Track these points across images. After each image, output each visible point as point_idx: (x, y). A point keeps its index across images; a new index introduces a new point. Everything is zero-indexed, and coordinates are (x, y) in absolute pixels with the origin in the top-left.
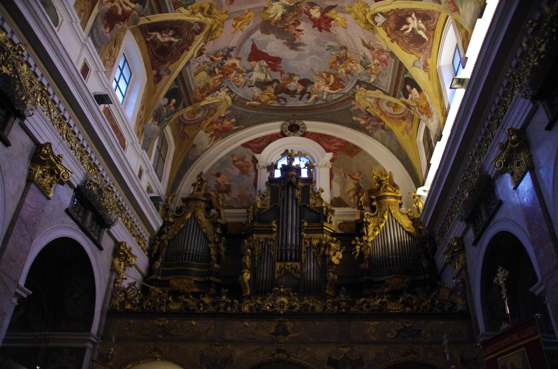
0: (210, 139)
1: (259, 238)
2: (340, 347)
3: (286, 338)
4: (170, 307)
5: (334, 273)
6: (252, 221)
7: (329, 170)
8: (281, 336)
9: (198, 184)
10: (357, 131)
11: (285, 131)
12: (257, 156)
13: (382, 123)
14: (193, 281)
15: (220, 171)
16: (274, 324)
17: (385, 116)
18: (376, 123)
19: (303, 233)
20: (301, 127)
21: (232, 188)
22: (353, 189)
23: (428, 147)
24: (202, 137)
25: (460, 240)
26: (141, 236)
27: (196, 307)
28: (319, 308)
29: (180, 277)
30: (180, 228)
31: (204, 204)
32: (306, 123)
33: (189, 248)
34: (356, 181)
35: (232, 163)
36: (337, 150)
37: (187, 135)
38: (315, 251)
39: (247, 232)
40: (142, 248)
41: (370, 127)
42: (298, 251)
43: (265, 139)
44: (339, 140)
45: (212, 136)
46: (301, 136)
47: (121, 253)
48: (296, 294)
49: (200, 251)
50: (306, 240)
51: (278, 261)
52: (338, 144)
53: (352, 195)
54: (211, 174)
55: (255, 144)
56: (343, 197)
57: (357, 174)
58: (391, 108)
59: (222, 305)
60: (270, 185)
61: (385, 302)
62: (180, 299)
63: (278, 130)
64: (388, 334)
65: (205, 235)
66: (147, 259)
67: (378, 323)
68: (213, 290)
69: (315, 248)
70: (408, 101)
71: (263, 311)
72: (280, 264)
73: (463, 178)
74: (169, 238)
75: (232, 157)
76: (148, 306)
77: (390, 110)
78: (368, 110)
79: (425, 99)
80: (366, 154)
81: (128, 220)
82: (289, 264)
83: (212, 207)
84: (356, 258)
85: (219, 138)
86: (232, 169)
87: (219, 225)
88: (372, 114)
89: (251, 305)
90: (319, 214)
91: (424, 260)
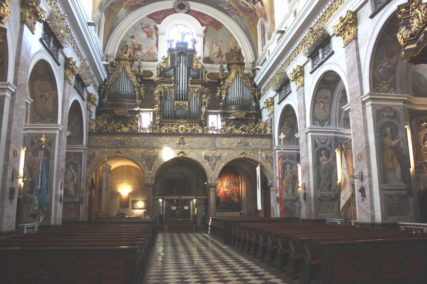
1: (164, 86)
5: (206, 108)
6: (160, 76)
9: (125, 49)
15: (134, 35)
16: (178, 139)
17: (240, 8)
18: (234, 11)
19: (189, 84)
21: (142, 47)
24: (123, 11)
25: (272, 99)
29: (120, 108)
32: (191, 3)
33: (123, 91)
34: (218, 47)
37: (113, 11)
38: (196, 95)
44: (210, 17)
45: (128, 10)
46: (185, 13)
50: (191, 89)
51: (175, 100)
52: (209, 20)
56: (210, 58)
57: (219, 42)
58: (244, 5)
60: (170, 53)
61: (233, 129)
62: (128, 126)
63: (171, 7)
65: (131, 82)
70: (255, 7)
72: (176, 102)
73: (277, 72)
75: (141, 24)
76: (110, 130)
77: (244, 6)
78: (230, 3)
79: (265, 10)
80: (226, 29)
82: (181, 102)
86: (142, 34)
88: (232, 5)
89: (166, 129)
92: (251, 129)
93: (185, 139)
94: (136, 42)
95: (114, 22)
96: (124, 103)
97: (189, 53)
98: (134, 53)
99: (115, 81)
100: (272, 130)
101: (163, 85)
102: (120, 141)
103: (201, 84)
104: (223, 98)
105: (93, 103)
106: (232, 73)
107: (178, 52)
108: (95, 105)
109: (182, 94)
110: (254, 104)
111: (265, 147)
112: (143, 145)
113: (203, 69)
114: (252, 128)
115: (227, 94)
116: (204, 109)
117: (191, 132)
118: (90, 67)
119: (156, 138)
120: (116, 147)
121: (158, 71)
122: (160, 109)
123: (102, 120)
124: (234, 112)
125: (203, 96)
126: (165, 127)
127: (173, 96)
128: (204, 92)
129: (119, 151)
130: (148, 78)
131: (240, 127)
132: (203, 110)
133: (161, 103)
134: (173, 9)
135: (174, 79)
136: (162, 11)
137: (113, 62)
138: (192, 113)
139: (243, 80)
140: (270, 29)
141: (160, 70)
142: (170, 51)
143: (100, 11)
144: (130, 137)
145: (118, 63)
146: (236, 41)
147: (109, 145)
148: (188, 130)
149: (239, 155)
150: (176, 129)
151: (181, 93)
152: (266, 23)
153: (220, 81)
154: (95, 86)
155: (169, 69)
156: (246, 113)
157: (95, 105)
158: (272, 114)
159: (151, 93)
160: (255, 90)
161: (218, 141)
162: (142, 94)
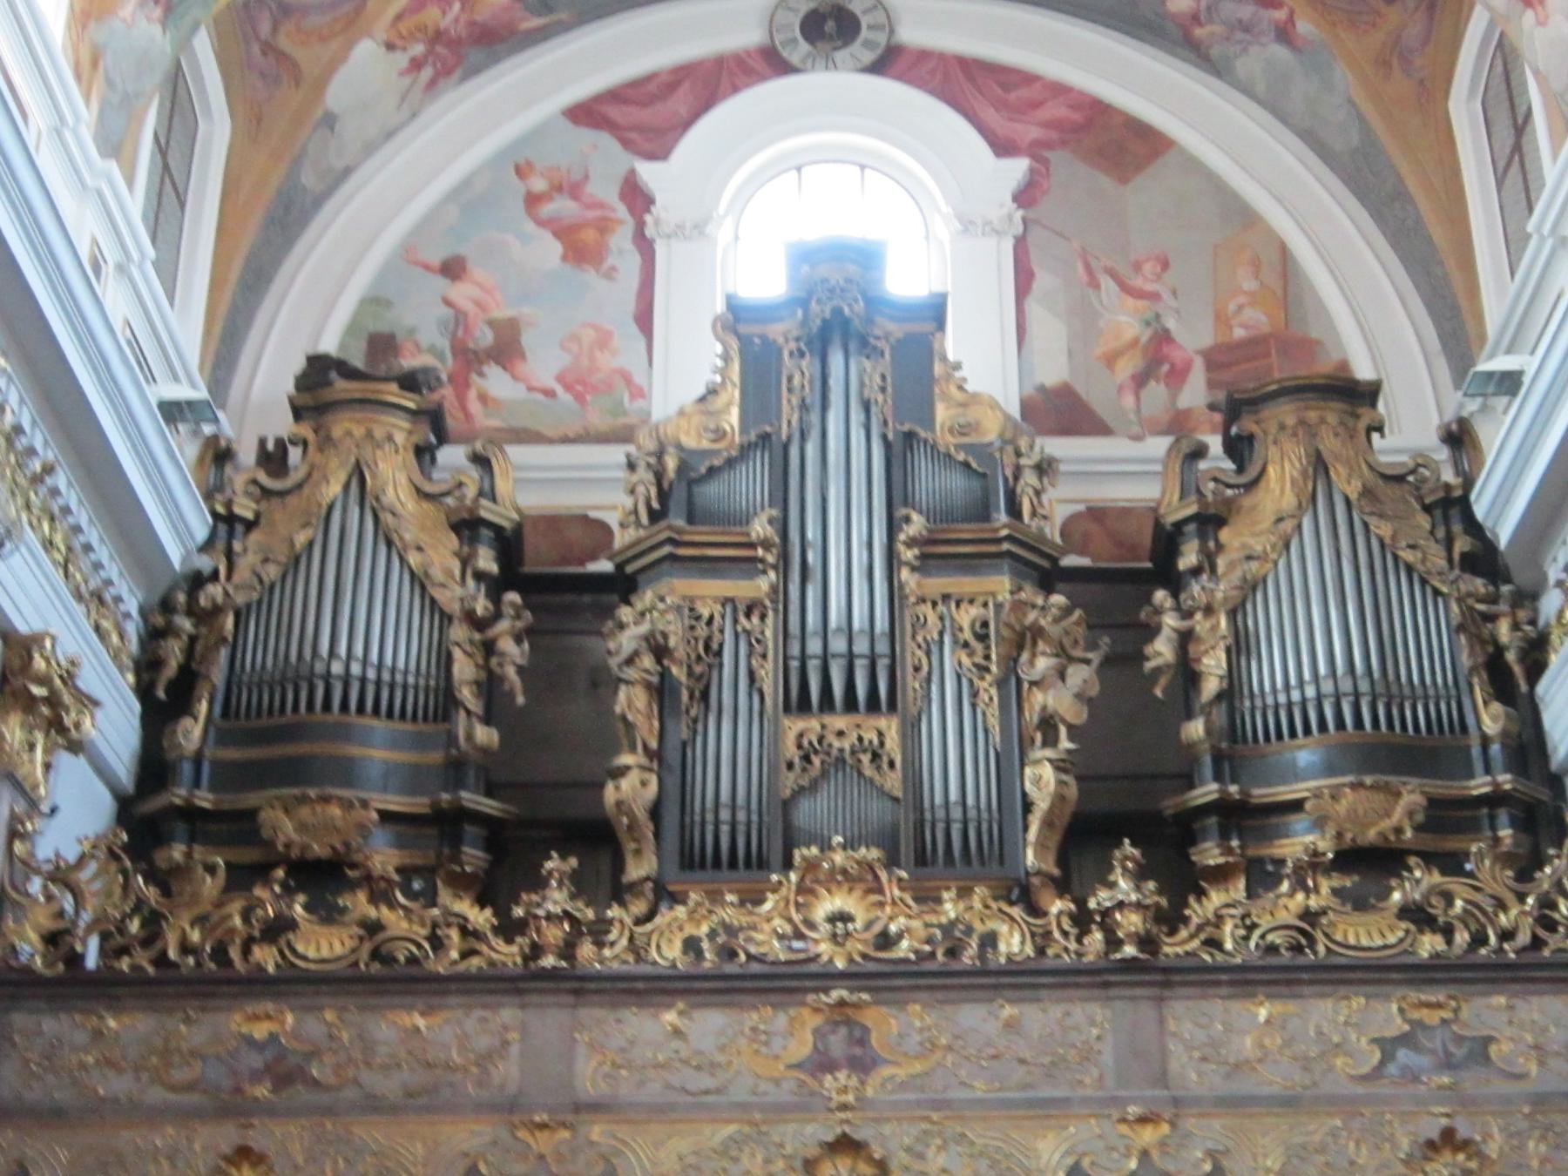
0: (407, 80)
1: (692, 600)
2: (1123, 1120)
3: (863, 1083)
4: (300, 948)
5: (1059, 766)
6: (655, 516)
7: (1008, 246)
8: (842, 1076)
10: (1147, 48)
11: (783, 44)
12: (648, 172)
13: (1280, 15)
14: (375, 816)
15: (462, 250)
19: (905, 574)
20: (865, 21)
21: (528, 339)
22: (1135, 343)
23: (1510, 142)
26: (108, 597)
27: (427, 946)
28: (1017, 938)
30: (292, 544)
31: (406, 425)
34: (1141, 303)
36: (1048, 145)
39: (629, 569)
40: (116, 658)
41: (1217, 28)
43: (686, 86)
44: (1059, 90)
45: (416, 65)
48: (904, 874)
49: (401, 664)
50: (927, 609)
51: (787, 708)
52: (1055, 110)
56: (1081, 389)
57: (1148, 268)
59: (554, 934)
60: (739, 337)
61: (1323, 912)
62: (343, 911)
63: (747, 36)
64: (1339, 1062)
65: (420, 582)
66: (137, 707)
67: (1292, 1007)
68: (473, 857)
69: (966, 645)
71: (750, 957)
74: (240, 599)
75: (521, 171)
80: (1194, 166)
81: (52, 519)
82: (839, 722)
83: (443, 438)
84: (1158, 692)
85: (443, 72)
89: (689, 930)
90: (984, 475)
91: (1485, 703)
92: (1502, 906)
93: (870, 1017)
94: (478, 304)
96: (355, 751)
97: (897, 330)
99: (284, 577)
102: (269, 1054)
103: (1006, 564)
104: (1211, 686)
106: (1272, 471)
107: (805, 322)
109: (851, 657)
110: (1491, 719)
112: (480, 1084)
113: (1023, 444)
114: (1509, 898)
115: (1240, 647)
116: (1048, 772)
117: (922, 957)
119: (599, 1013)
120: (233, 1108)
121: (644, 475)
124: (1317, 794)
125: (1032, 663)
126: (681, 911)
127: (768, 675)
128: (1037, 632)
129: (257, 1139)
131: (1390, 890)
132: (1037, 781)
135: (769, 528)
136: (682, 74)
138: (940, 814)
139: (1373, 522)
141: (659, 476)
142: (737, 319)
143: (158, 12)
144: (362, 1009)
146: (1284, 251)
147: (173, 1088)
148: (900, 936)
149: (1407, 1162)
154: (97, 599)
155: (730, 463)
156: (1434, 803)
157: (75, 747)
159: (594, 685)
160: (1493, 599)
161: (1187, 1028)
162: (511, 672)
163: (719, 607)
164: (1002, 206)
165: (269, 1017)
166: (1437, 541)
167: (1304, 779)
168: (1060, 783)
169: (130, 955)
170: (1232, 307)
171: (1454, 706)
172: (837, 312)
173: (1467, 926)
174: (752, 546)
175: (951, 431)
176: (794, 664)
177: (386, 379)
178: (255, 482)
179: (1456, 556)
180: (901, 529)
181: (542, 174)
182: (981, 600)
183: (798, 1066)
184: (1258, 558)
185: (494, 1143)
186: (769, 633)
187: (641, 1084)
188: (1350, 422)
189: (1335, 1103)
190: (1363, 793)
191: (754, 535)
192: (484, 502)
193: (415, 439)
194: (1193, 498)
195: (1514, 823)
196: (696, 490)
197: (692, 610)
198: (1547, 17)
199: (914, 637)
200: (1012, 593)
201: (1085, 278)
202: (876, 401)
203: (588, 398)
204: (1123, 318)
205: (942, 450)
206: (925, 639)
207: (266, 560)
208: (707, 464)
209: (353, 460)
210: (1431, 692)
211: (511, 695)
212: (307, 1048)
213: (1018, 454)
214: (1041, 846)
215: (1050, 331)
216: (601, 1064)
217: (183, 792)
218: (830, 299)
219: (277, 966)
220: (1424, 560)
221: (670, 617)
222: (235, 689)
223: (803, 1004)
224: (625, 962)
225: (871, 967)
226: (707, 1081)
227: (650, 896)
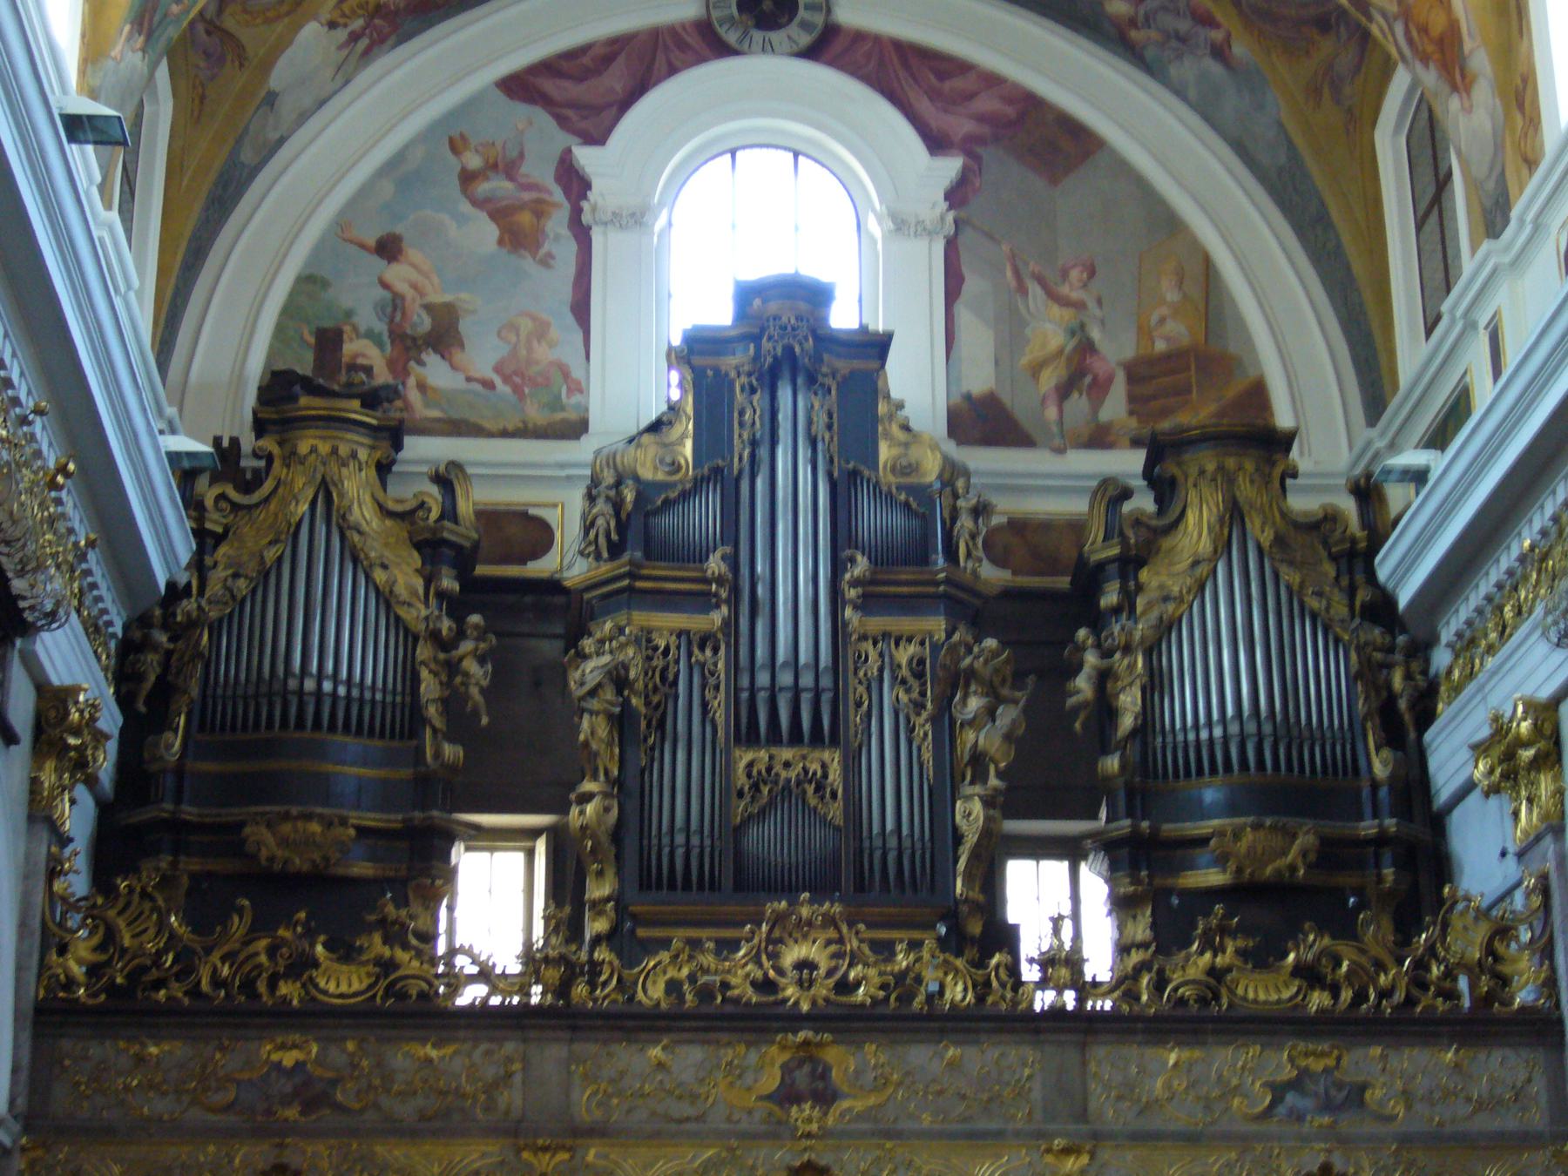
0: (345, 52)
1: (650, 632)
2: (1049, 1151)
3: (826, 1114)
4: (322, 984)
5: (988, 803)
8: (807, 1106)
10: (1084, 42)
12: (587, 157)
13: (1217, 35)
14: (352, 832)
15: (399, 229)
18: (1184, 25)
19: (848, 612)
21: (465, 326)
22: (1060, 352)
23: (1431, 191)
26: (101, 623)
28: (960, 987)
29: (295, 811)
34: (1067, 314)
35: (457, 182)
37: (239, 48)
38: (904, 697)
39: (587, 596)
41: (1154, 34)
42: (826, 698)
43: (621, 60)
44: (992, 81)
45: (354, 37)
47: (72, 741)
50: (868, 646)
51: (738, 741)
52: (987, 103)
53: (1053, 382)
54: (351, 242)
55: (566, 84)
56: (1006, 398)
57: (1074, 274)
60: (693, 368)
61: (1229, 969)
62: (361, 950)
64: (1236, 1102)
65: (385, 599)
67: (1197, 1053)
69: (904, 682)
72: (748, 756)
74: (213, 614)
75: (456, 146)
80: (1123, 169)
82: (786, 754)
84: (1077, 725)
85: (382, 40)
87: (446, 551)
89: (671, 973)
90: (924, 515)
91: (1377, 750)
92: (1380, 966)
94: (414, 287)
95: (246, 128)
96: (330, 768)
97: (844, 366)
98: (399, 367)
99: (254, 592)
100: (1553, 969)
101: (642, 618)
104: (1127, 722)
105: (80, 766)
106: (1191, 517)
107: (757, 358)
108: (91, 782)
109: (796, 690)
110: (1381, 765)
111: (1509, 1122)
112: (487, 1109)
113: (960, 484)
114: (1388, 960)
115: (1156, 684)
116: (977, 807)
117: (875, 1002)
118: (67, 475)
119: (592, 1048)
121: (601, 506)
122: (615, 812)
123: (147, 905)
124: (1220, 833)
126: (665, 956)
128: (971, 674)
130: (512, 571)
131: (1286, 955)
133: (621, 769)
134: (705, 28)
135: (724, 568)
136: (617, 46)
137: (235, 442)
138: (878, 843)
140: (1499, 147)
141: (617, 505)
143: (141, 39)
145: (276, 450)
148: (858, 984)
150: (759, 974)
151: (785, 679)
152: (1455, 103)
153: (1089, 578)
154: (94, 629)
155: (685, 496)
156: (1326, 842)
157: (91, 782)
158: (1548, 844)
159: (537, 684)
160: (1390, 650)
162: (474, 691)
163: (674, 638)
164: (934, 205)
165: (295, 1046)
166: (1341, 589)
167: (1210, 818)
168: (988, 819)
169: (167, 988)
170: (1154, 318)
171: (1348, 747)
172: (789, 350)
173: (1351, 985)
174: (707, 581)
175: (893, 470)
176: (745, 695)
177: (351, 396)
178: (222, 497)
179: (1358, 603)
180: (845, 570)
181: (477, 151)
182: (917, 639)
183: (769, 1097)
184: (1175, 599)
185: (502, 1163)
186: (721, 665)
187: (629, 1111)
188: (1267, 470)
189: (1227, 1138)
190: (1261, 834)
191: (709, 572)
192: (446, 523)
193: (378, 455)
194: (1116, 540)
195: (1394, 864)
196: (653, 521)
197: (649, 641)
198: (1471, 106)
199: (856, 673)
200: (949, 635)
201: (1013, 283)
202: (823, 439)
203: (527, 391)
204: (1048, 326)
205: (885, 489)
206: (865, 675)
207: (236, 576)
208: (663, 496)
209: (319, 477)
210: (1328, 734)
211: (476, 714)
212: (330, 1075)
213: (956, 496)
214: (969, 877)
215: (978, 338)
216: (594, 1094)
217: (168, 806)
218: (782, 337)
219: (300, 1001)
220: (1328, 609)
221: (631, 651)
222: (210, 702)
223: (773, 1042)
224: (614, 1002)
225: (831, 1010)
226: (687, 1110)
227: (613, 914)
